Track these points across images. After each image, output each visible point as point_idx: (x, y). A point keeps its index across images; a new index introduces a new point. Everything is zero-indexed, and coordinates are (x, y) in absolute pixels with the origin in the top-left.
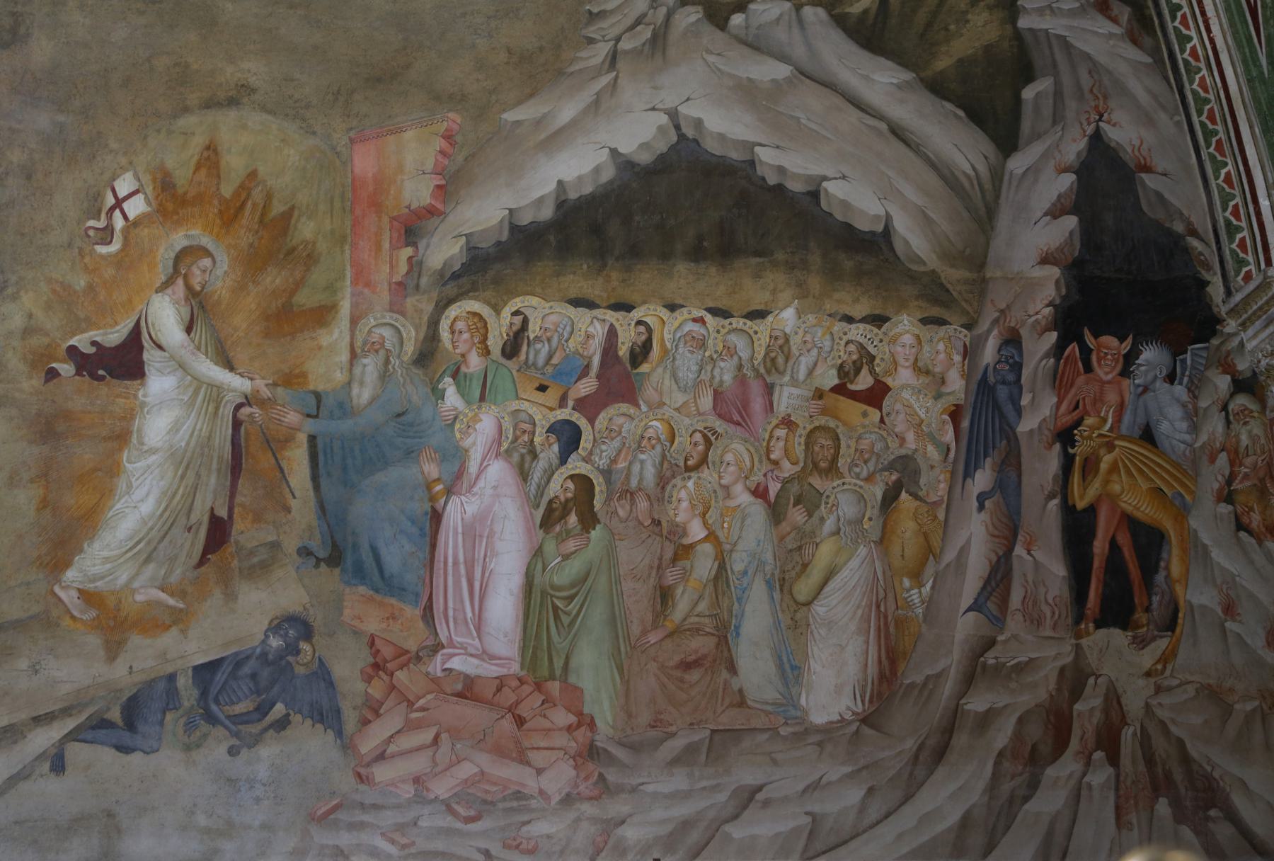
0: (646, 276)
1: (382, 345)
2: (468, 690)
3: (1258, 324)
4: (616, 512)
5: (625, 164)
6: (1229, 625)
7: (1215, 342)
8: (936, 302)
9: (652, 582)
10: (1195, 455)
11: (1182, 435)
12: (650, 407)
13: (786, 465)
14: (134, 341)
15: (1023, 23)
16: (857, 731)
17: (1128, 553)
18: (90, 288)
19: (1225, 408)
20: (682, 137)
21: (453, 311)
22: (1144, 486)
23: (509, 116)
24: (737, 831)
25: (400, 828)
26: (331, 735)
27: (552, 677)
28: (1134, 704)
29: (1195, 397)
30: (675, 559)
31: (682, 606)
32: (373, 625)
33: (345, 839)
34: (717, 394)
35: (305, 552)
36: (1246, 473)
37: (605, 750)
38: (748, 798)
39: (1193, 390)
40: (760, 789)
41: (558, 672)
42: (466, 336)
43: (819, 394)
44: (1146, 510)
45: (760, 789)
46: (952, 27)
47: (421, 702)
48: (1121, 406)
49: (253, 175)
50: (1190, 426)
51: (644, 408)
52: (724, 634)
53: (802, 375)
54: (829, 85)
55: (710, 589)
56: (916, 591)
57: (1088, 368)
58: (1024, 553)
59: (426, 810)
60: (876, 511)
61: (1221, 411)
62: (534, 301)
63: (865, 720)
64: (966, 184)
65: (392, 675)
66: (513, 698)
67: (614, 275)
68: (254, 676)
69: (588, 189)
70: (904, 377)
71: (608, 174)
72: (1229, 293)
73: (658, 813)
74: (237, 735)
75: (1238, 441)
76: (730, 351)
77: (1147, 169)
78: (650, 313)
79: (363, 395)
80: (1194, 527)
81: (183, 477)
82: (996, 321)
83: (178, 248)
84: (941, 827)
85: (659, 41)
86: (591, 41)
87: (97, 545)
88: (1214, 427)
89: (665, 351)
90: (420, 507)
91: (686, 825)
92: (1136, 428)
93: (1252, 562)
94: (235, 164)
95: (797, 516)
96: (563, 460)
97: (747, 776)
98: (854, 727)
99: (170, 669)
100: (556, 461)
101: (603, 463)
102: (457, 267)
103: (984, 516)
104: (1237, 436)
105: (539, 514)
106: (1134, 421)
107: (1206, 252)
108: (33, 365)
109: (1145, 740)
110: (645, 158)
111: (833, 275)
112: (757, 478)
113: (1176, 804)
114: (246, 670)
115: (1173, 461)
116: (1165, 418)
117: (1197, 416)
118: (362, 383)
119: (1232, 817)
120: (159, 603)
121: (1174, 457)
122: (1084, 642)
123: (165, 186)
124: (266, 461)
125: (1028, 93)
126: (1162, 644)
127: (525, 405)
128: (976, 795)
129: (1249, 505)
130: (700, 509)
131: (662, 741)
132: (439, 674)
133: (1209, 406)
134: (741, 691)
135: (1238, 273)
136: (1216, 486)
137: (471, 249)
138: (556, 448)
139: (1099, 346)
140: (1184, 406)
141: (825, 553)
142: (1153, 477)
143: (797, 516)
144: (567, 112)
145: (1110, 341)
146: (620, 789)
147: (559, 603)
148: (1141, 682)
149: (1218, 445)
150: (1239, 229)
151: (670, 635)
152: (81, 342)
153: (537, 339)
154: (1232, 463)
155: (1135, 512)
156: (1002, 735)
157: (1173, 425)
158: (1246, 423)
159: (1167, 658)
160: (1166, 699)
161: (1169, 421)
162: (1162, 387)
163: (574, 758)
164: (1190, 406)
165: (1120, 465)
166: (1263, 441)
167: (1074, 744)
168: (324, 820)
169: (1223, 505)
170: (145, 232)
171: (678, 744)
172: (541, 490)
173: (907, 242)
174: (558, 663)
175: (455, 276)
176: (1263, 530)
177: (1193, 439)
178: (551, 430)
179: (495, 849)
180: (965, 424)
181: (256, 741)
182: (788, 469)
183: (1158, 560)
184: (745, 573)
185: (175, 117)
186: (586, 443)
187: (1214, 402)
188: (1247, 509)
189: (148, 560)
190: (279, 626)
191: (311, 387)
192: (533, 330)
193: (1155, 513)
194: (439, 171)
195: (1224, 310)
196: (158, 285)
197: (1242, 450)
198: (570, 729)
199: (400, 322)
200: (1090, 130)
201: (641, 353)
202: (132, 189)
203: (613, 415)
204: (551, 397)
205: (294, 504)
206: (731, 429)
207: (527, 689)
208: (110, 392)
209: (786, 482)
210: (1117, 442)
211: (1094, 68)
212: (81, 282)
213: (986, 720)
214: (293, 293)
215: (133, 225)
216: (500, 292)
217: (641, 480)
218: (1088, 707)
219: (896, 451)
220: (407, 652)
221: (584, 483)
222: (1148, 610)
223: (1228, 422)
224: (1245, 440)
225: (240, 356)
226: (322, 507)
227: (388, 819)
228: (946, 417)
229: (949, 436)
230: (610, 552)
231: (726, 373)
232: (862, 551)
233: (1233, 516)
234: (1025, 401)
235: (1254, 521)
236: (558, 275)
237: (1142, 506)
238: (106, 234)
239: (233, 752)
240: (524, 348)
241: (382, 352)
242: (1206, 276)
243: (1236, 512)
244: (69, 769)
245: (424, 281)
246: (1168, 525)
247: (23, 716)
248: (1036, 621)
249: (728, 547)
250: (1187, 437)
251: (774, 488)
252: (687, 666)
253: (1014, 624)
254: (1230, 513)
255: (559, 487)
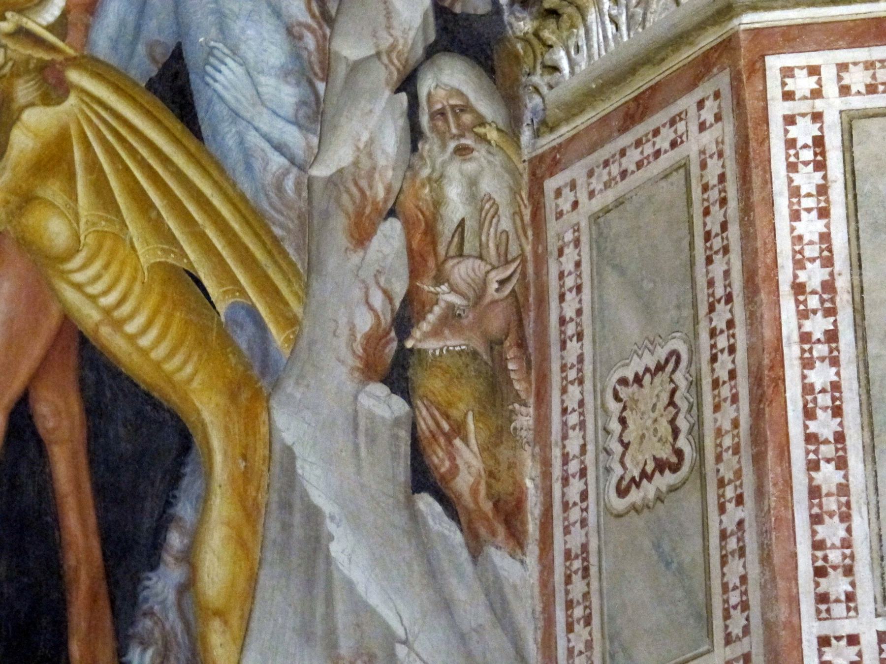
10: (310, 200)
11: (280, 124)
29: (327, 19)
36: (451, 307)
50: (302, 103)
61: (398, 90)
75: (438, 203)
80: (288, 437)
92: (141, 49)
93: (446, 606)
104: (437, 181)
106: (138, 28)
115: (243, 197)
116: (235, 52)
117: (326, 79)
121: (246, 186)
129: (455, 413)
133: (367, 59)
136: (364, 323)
140: (292, 33)
142: (177, 234)
149: (381, 194)
155: (105, 331)
157: (255, 85)
158: (462, 151)
161: (243, 63)
164: (310, 41)
165: (78, 155)
166: (505, 224)
169: (380, 390)
176: (487, 506)
177: (309, 147)
187: (378, 55)
188: (446, 427)
193: (171, 355)
197: (446, 229)
210: (74, 76)
223: (415, 134)
233: (404, 435)
235: (462, 466)
237: (131, 317)
243: (414, 426)
254: (397, 422)
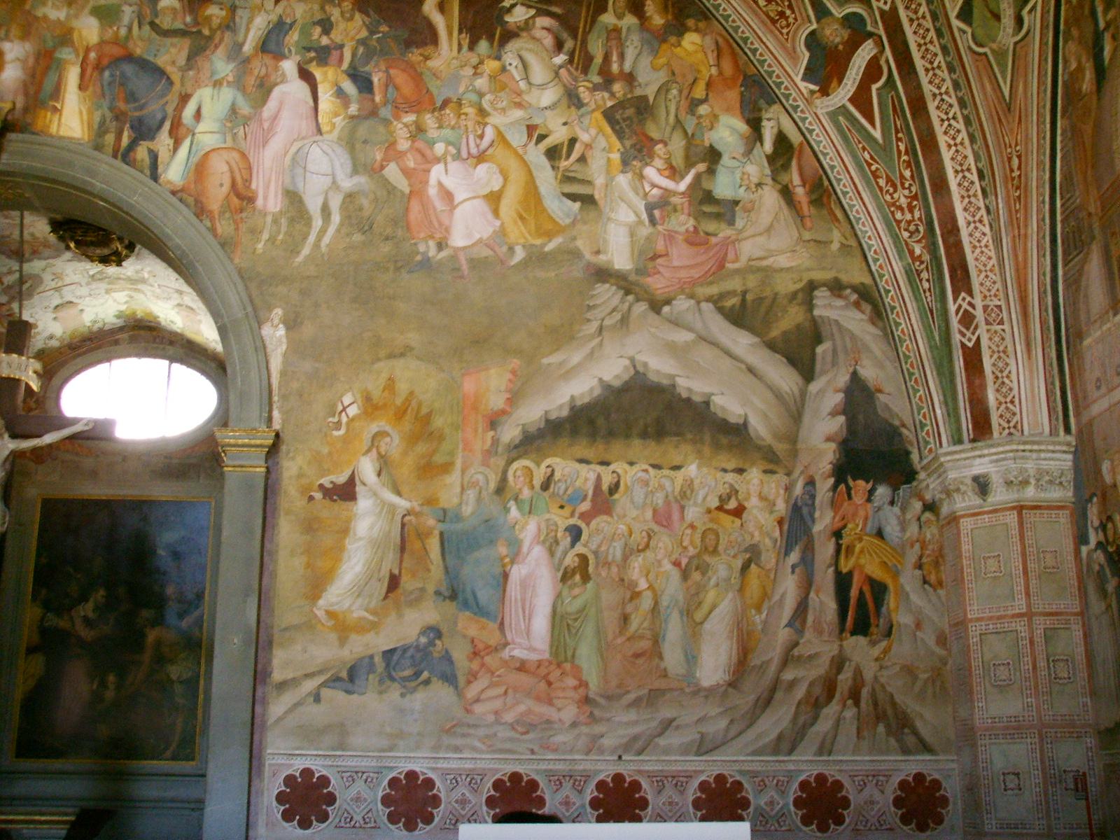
0: (617, 447)
1: (478, 484)
2: (522, 667)
3: (935, 475)
4: (600, 575)
5: (606, 387)
6: (918, 633)
7: (915, 484)
8: (771, 461)
9: (619, 611)
12: (619, 518)
13: (691, 549)
14: (351, 482)
15: (816, 312)
16: (726, 690)
17: (868, 596)
18: (330, 454)
19: (919, 519)
20: (637, 372)
21: (515, 465)
22: (877, 560)
23: (545, 361)
24: (662, 741)
25: (487, 736)
26: (451, 689)
27: (566, 660)
28: (868, 675)
30: (632, 599)
31: (634, 625)
32: (473, 631)
33: (459, 742)
34: (655, 511)
35: (438, 593)
37: (594, 700)
38: (667, 725)
39: (904, 509)
40: (674, 719)
41: (569, 658)
42: (522, 479)
43: (709, 511)
44: (877, 573)
45: (674, 719)
46: (780, 314)
47: (498, 673)
48: (866, 519)
49: (412, 393)
51: (616, 518)
52: (656, 641)
53: (700, 498)
54: (714, 344)
55: (649, 616)
56: (757, 617)
57: (850, 497)
58: (815, 597)
59: (500, 728)
60: (738, 575)
62: (558, 460)
63: (732, 684)
64: (786, 396)
65: (483, 658)
66: (546, 671)
67: (601, 447)
68: (412, 657)
69: (586, 400)
70: (753, 503)
71: (597, 392)
72: (921, 458)
73: (621, 732)
74: (404, 687)
76: (662, 487)
77: (880, 391)
78: (619, 466)
79: (467, 510)
81: (376, 553)
82: (802, 473)
83: (373, 432)
84: (767, 740)
85: (624, 321)
86: (589, 320)
87: (333, 588)
88: (913, 530)
89: (627, 486)
90: (497, 570)
91: (635, 738)
93: (930, 601)
94: (403, 387)
95: (696, 576)
96: (573, 545)
97: (667, 713)
98: (724, 688)
99: (370, 652)
100: (568, 546)
101: (594, 547)
102: (517, 441)
103: (795, 577)
105: (560, 574)
107: (911, 436)
108: (302, 493)
109: (873, 694)
110: (617, 383)
111: (717, 446)
112: (674, 557)
113: (888, 727)
114: (409, 654)
118: (467, 504)
119: (916, 733)
120: (364, 618)
122: (845, 643)
123: (368, 399)
124: (418, 545)
125: (819, 350)
126: (884, 644)
127: (553, 516)
128: (785, 723)
130: (644, 573)
131: (625, 694)
132: (507, 658)
134: (665, 669)
135: (925, 448)
136: (914, 561)
137: (524, 432)
138: (569, 539)
139: (855, 486)
140: (898, 518)
141: (711, 596)
143: (696, 576)
144: (576, 358)
145: (861, 483)
146: (601, 719)
147: (570, 622)
148: (873, 664)
150: (926, 425)
151: (629, 639)
152: (326, 481)
153: (559, 480)
154: (922, 548)
156: (800, 693)
159: (886, 651)
160: (885, 673)
162: (887, 508)
163: (577, 703)
167: (838, 696)
168: (448, 731)
170: (357, 424)
171: (632, 696)
172: (561, 561)
173: (756, 430)
174: (569, 654)
175: (516, 447)
178: (566, 529)
179: (536, 749)
180: (786, 527)
181: (414, 690)
182: (692, 551)
183: (883, 600)
184: (668, 607)
185: (373, 363)
186: (584, 537)
189: (358, 596)
190: (425, 632)
191: (441, 505)
192: (557, 476)
194: (508, 390)
195: (917, 466)
196: (364, 451)
198: (575, 688)
199: (487, 471)
200: (851, 370)
201: (614, 488)
202: (351, 401)
203: (600, 521)
204: (567, 511)
205: (433, 568)
206: (662, 529)
207: (553, 667)
208: (340, 507)
209: (691, 558)
210: (865, 537)
211: (853, 337)
212: (325, 450)
213: (792, 684)
214: (431, 457)
215: (351, 420)
216: (540, 456)
217: (614, 557)
218: (845, 678)
219: (748, 541)
220: (490, 646)
221: (584, 559)
222: (877, 626)
223: (920, 527)
224: (929, 536)
225: (405, 489)
226: (446, 570)
227: (481, 732)
228: (776, 523)
229: (777, 534)
230: (597, 597)
231: (659, 499)
232: (730, 595)
234: (817, 514)
236: (570, 445)
238: (338, 425)
239: (403, 695)
240: (552, 486)
241: (478, 488)
242: (910, 449)
244: (322, 702)
245: (500, 449)
246: (889, 582)
247: (299, 674)
248: (820, 632)
249: (659, 593)
250: (900, 535)
251: (684, 562)
252: (637, 656)
253: (809, 634)
255: (571, 560)
